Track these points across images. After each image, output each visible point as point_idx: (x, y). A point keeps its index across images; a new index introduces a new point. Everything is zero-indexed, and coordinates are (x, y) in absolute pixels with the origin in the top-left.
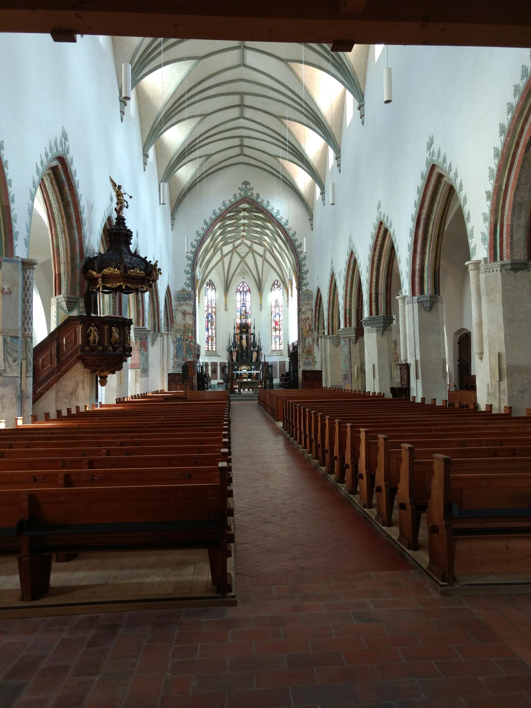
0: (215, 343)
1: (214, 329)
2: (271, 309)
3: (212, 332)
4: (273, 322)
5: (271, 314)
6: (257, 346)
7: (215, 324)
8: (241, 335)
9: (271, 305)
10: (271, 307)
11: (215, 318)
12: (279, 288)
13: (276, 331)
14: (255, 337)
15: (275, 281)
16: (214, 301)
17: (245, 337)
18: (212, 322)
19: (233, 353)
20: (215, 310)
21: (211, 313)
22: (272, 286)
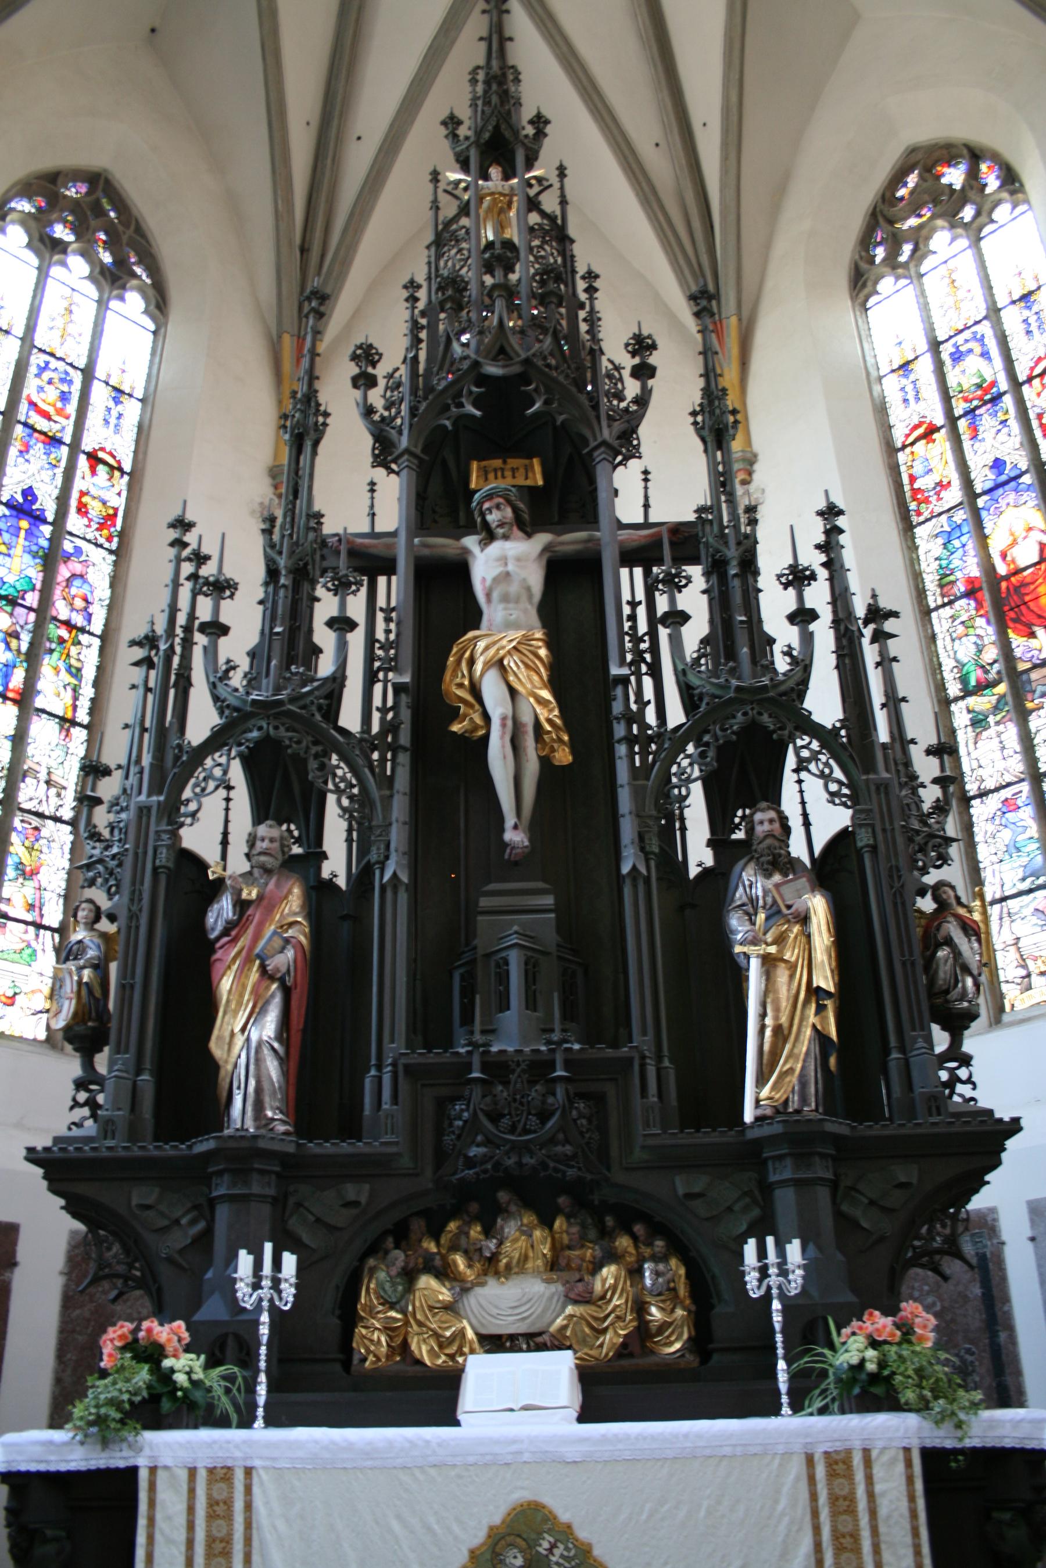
0: (54, 915)
1: (67, 723)
2: (894, 470)
3: (19, 739)
4: (941, 621)
5: (908, 527)
6: (826, 736)
7: (89, 657)
8: (443, 545)
9: (886, 428)
10: (891, 450)
11: (102, 592)
12: (968, 213)
13: (1022, 716)
14: (749, 566)
15: (898, 178)
16: (132, 410)
17: (535, 578)
18: (43, 611)
19: (223, 910)
20: (119, 502)
21: (48, 506)
22: (866, 242)
